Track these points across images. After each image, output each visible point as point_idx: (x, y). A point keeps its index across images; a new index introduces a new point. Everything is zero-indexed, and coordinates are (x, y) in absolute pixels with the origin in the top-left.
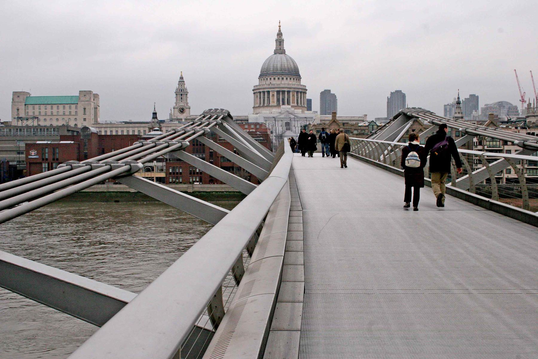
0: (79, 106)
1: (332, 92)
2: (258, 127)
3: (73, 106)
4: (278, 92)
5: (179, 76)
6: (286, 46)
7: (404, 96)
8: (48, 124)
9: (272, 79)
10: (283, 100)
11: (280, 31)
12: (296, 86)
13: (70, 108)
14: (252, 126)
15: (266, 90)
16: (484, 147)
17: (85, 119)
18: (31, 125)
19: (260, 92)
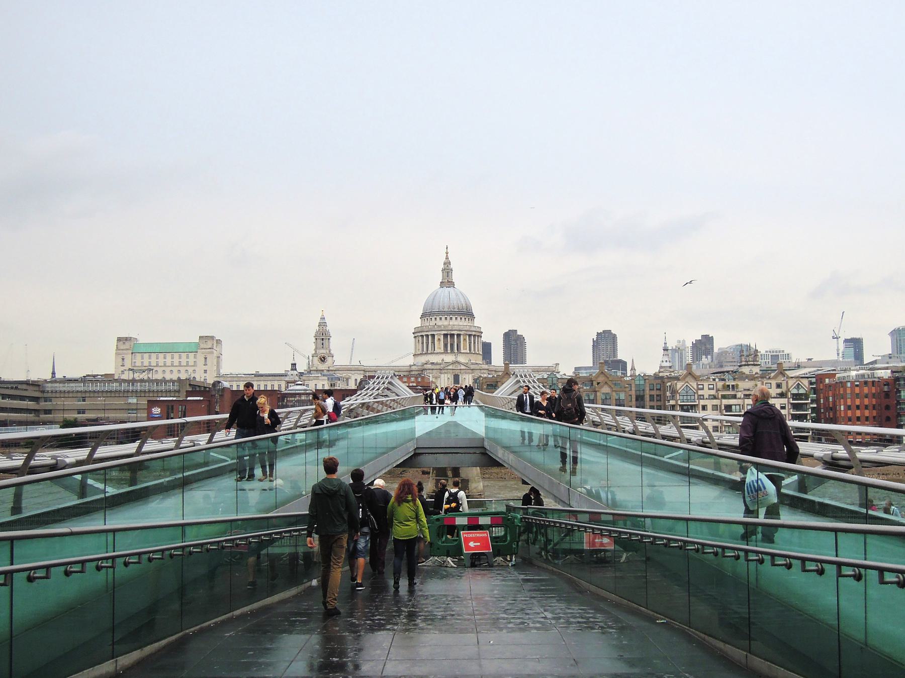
0: (198, 355)
1: (519, 333)
2: (419, 380)
3: (191, 355)
4: (445, 336)
5: (320, 316)
6: (455, 277)
7: (614, 338)
8: (159, 376)
9: (438, 318)
10: (452, 345)
11: (447, 258)
12: (468, 328)
13: (188, 357)
14: (413, 379)
15: (429, 333)
16: (677, 402)
17: (205, 371)
18: (146, 378)
19: (422, 336)
